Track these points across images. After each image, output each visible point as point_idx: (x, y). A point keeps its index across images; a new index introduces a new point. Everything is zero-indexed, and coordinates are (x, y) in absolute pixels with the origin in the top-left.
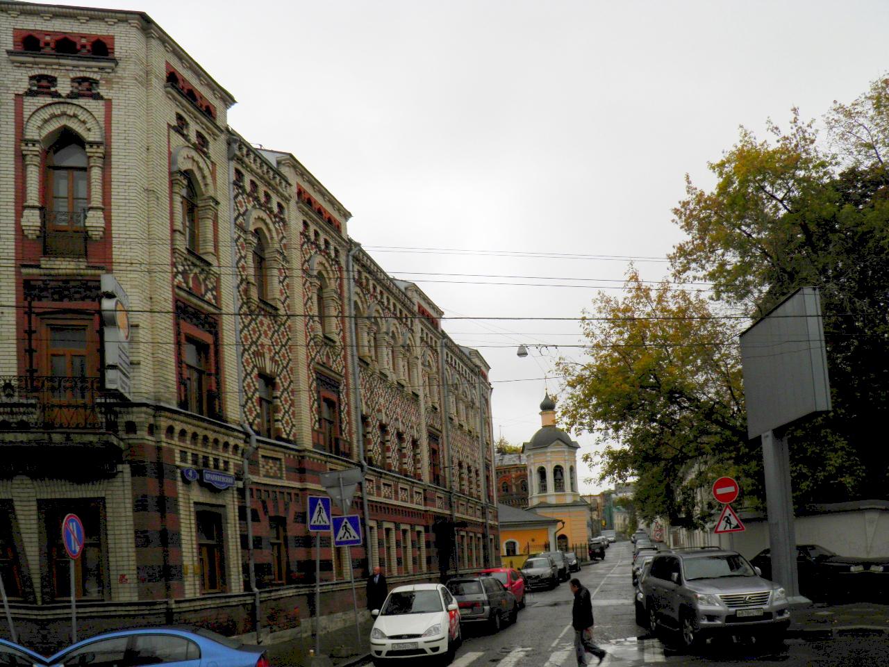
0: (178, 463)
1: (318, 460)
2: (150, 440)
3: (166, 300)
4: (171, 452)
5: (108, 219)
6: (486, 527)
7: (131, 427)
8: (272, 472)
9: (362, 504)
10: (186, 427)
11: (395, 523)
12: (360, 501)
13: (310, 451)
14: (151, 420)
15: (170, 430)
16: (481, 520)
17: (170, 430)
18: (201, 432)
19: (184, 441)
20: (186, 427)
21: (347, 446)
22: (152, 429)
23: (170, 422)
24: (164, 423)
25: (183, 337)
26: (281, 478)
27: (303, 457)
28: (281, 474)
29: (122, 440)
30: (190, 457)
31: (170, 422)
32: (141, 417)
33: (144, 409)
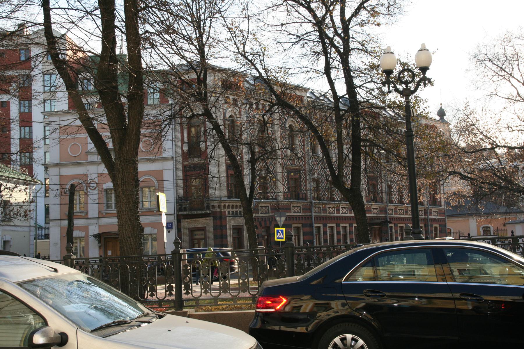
0: (227, 215)
1: (286, 204)
2: (218, 209)
3: (223, 166)
4: (225, 212)
5: (206, 144)
6: (427, 220)
7: (213, 206)
8: (264, 211)
9: (312, 218)
10: (229, 204)
11: (336, 224)
12: (310, 217)
13: (283, 202)
14: (219, 204)
15: (225, 206)
16: (423, 217)
17: (225, 206)
18: (235, 204)
19: (229, 208)
20: (229, 204)
21: (304, 195)
22: (219, 207)
23: (225, 204)
24: (222, 204)
25: (229, 176)
26: (269, 213)
27: (279, 204)
28: (269, 211)
29: (210, 210)
30: (231, 213)
31: (225, 204)
32: (215, 203)
33: (216, 201)
